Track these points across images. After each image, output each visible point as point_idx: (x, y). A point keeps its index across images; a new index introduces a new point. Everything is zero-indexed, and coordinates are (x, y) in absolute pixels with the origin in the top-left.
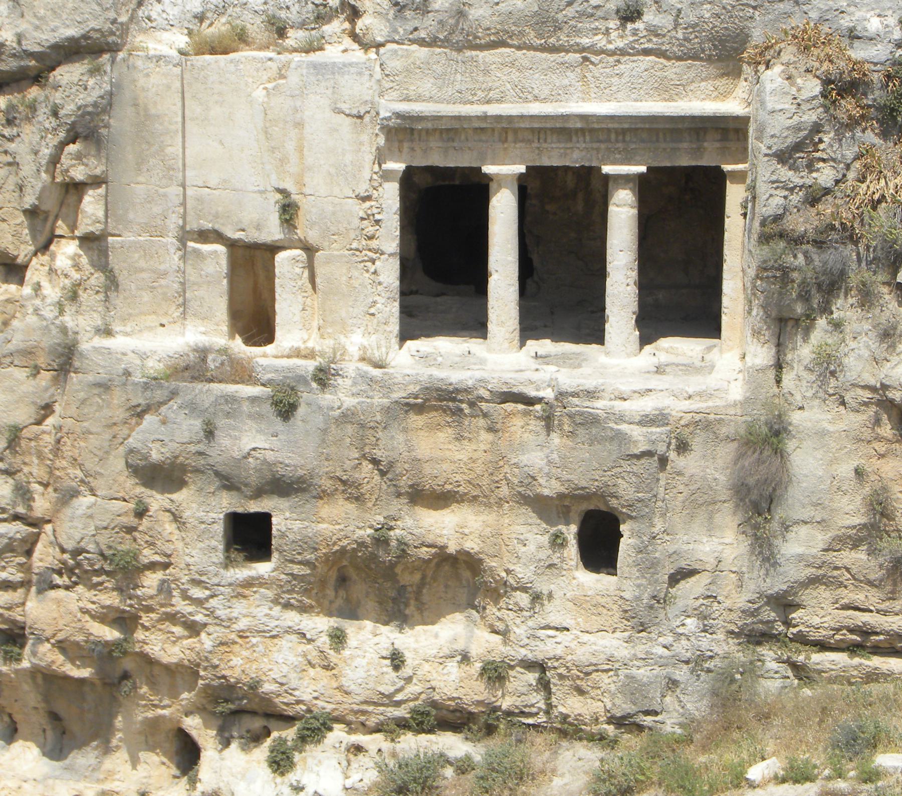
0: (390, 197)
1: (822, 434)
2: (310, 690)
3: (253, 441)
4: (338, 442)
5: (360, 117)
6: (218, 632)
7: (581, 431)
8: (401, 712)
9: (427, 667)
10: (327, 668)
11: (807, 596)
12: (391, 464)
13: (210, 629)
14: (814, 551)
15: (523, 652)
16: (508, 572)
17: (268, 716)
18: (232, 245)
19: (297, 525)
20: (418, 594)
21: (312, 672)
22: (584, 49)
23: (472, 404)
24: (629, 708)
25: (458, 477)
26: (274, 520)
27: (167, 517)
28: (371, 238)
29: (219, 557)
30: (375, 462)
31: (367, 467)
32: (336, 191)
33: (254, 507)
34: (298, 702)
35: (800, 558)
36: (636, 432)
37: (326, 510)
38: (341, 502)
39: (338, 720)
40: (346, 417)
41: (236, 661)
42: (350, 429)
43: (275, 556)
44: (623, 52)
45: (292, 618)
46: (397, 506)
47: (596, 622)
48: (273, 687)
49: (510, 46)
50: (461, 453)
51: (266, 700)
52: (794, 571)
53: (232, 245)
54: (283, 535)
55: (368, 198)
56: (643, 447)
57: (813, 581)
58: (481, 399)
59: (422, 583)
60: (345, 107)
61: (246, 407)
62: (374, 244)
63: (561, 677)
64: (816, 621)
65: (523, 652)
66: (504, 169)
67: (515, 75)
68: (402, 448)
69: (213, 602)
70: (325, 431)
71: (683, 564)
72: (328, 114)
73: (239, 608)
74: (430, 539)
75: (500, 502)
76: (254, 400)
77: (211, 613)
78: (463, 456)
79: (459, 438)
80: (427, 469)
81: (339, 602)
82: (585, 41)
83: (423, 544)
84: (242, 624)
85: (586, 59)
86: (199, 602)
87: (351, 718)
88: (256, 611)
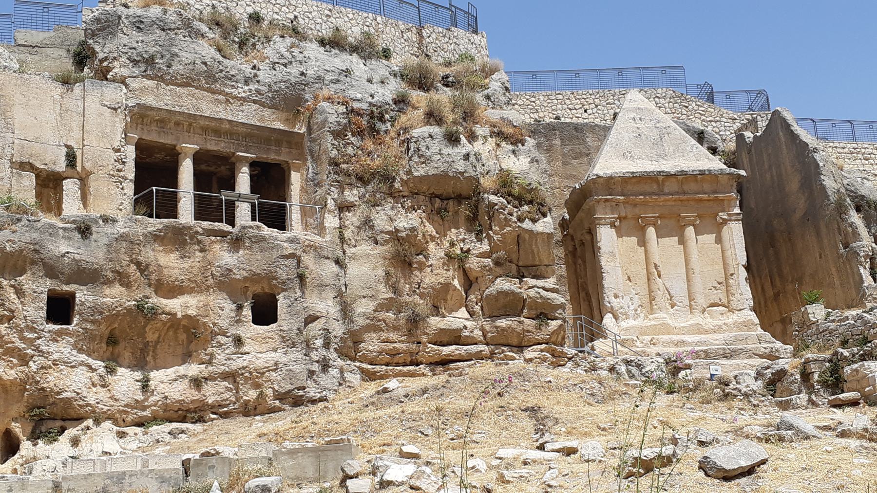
0: (130, 152)
1: (368, 255)
2: (94, 397)
3: (65, 248)
4: (117, 251)
5: (115, 109)
6: (40, 361)
7: (255, 246)
8: (147, 413)
9: (162, 385)
10: (103, 386)
11: (367, 336)
12: (147, 266)
13: (36, 358)
14: (369, 311)
15: (223, 368)
16: (214, 324)
17: (64, 420)
18: (38, 173)
19: (91, 298)
20: (155, 347)
21: (94, 389)
22: (227, 94)
23: (191, 238)
24: (289, 387)
25: (183, 277)
26: (77, 295)
27: (12, 290)
28: (119, 171)
29: (43, 314)
30: (138, 264)
31: (133, 267)
32: (102, 144)
33: (66, 288)
34: (88, 405)
35: (364, 314)
36: (286, 244)
37: (107, 291)
38: (118, 286)
39: (109, 418)
40: (123, 237)
41: (50, 378)
42: (124, 244)
43: (75, 320)
44: (244, 99)
45: (83, 357)
46: (149, 291)
47: (264, 347)
48: (74, 395)
49: (193, 86)
50: (187, 264)
51: (68, 400)
52: (361, 322)
53: (38, 173)
54: (83, 303)
55: (118, 151)
56: (291, 251)
57: (369, 328)
58: (197, 233)
59: (157, 342)
60: (107, 103)
61: (61, 232)
62: (121, 174)
63: (246, 379)
64: (371, 348)
65: (223, 368)
66: (190, 147)
67: (194, 101)
68: (152, 258)
69: (39, 342)
70: (109, 245)
71: (311, 313)
72: (98, 105)
73: (53, 347)
74: (167, 310)
75: (208, 288)
76: (65, 229)
77: (37, 349)
78: (186, 266)
79: (183, 257)
80: (166, 272)
81: (108, 354)
82: (227, 90)
83: (163, 313)
84: (55, 356)
85: (227, 100)
86: (30, 342)
87: (118, 415)
88: (63, 349)
